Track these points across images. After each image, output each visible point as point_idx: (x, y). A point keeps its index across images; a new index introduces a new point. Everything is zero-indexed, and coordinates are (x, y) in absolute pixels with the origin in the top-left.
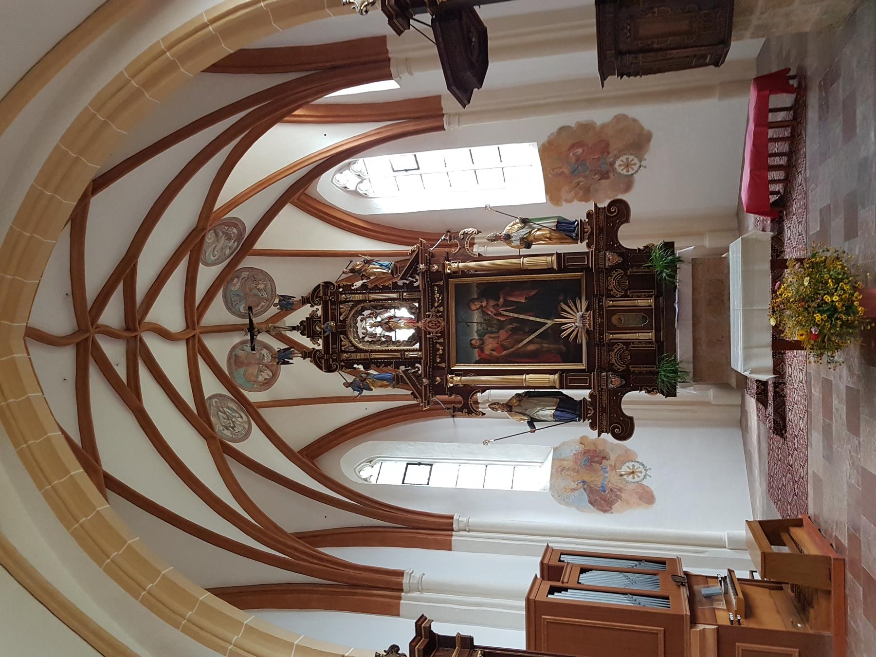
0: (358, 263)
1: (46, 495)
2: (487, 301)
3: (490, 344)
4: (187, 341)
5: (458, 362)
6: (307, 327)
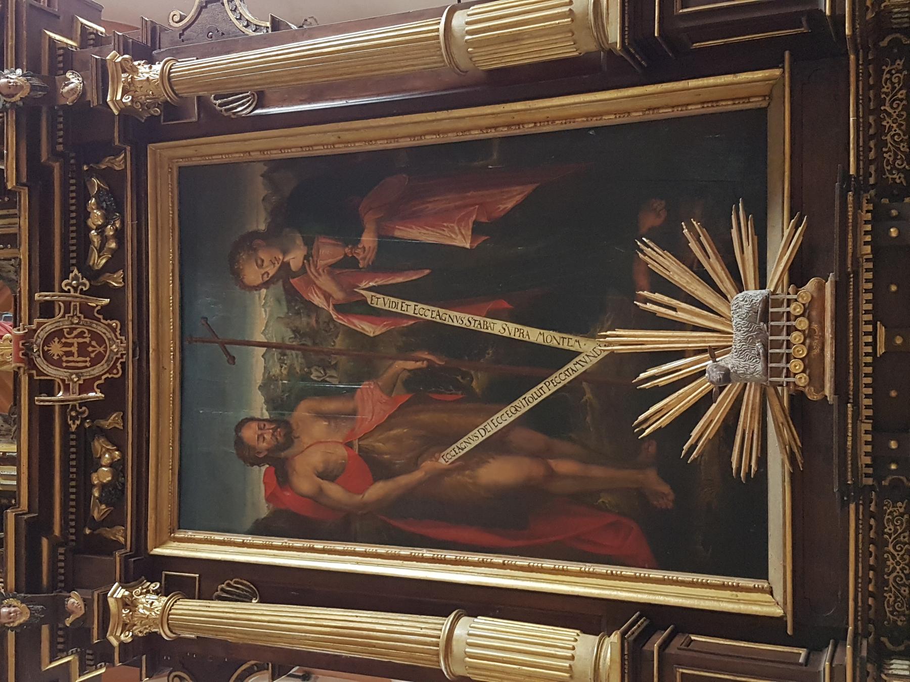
2: (309, 243)
3: (319, 446)
5: (186, 519)
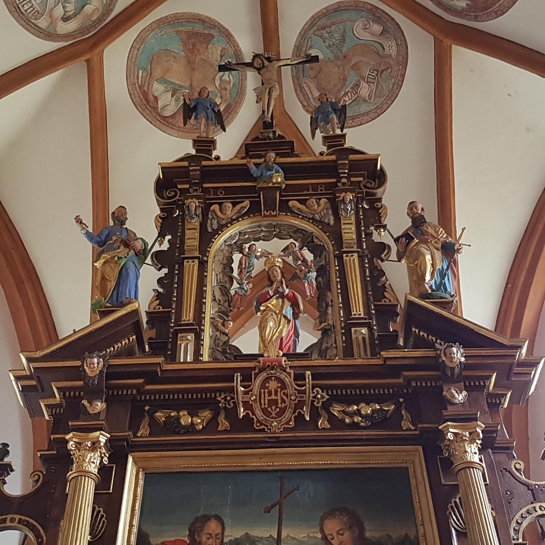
5: (152, 479)
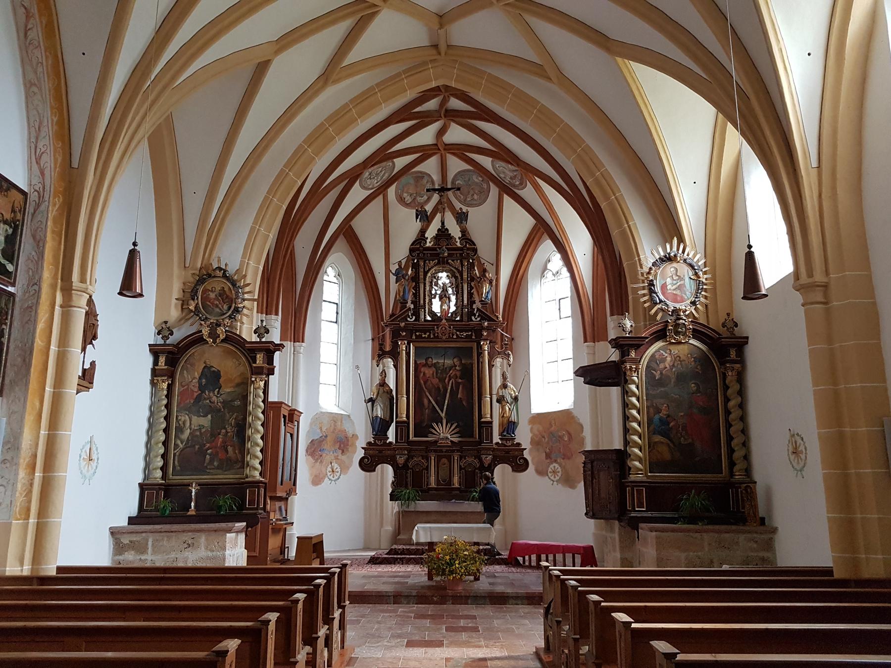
0: (490, 275)
1: (346, 105)
3: (429, 372)
4: (436, 145)
5: (416, 348)
6: (443, 233)
